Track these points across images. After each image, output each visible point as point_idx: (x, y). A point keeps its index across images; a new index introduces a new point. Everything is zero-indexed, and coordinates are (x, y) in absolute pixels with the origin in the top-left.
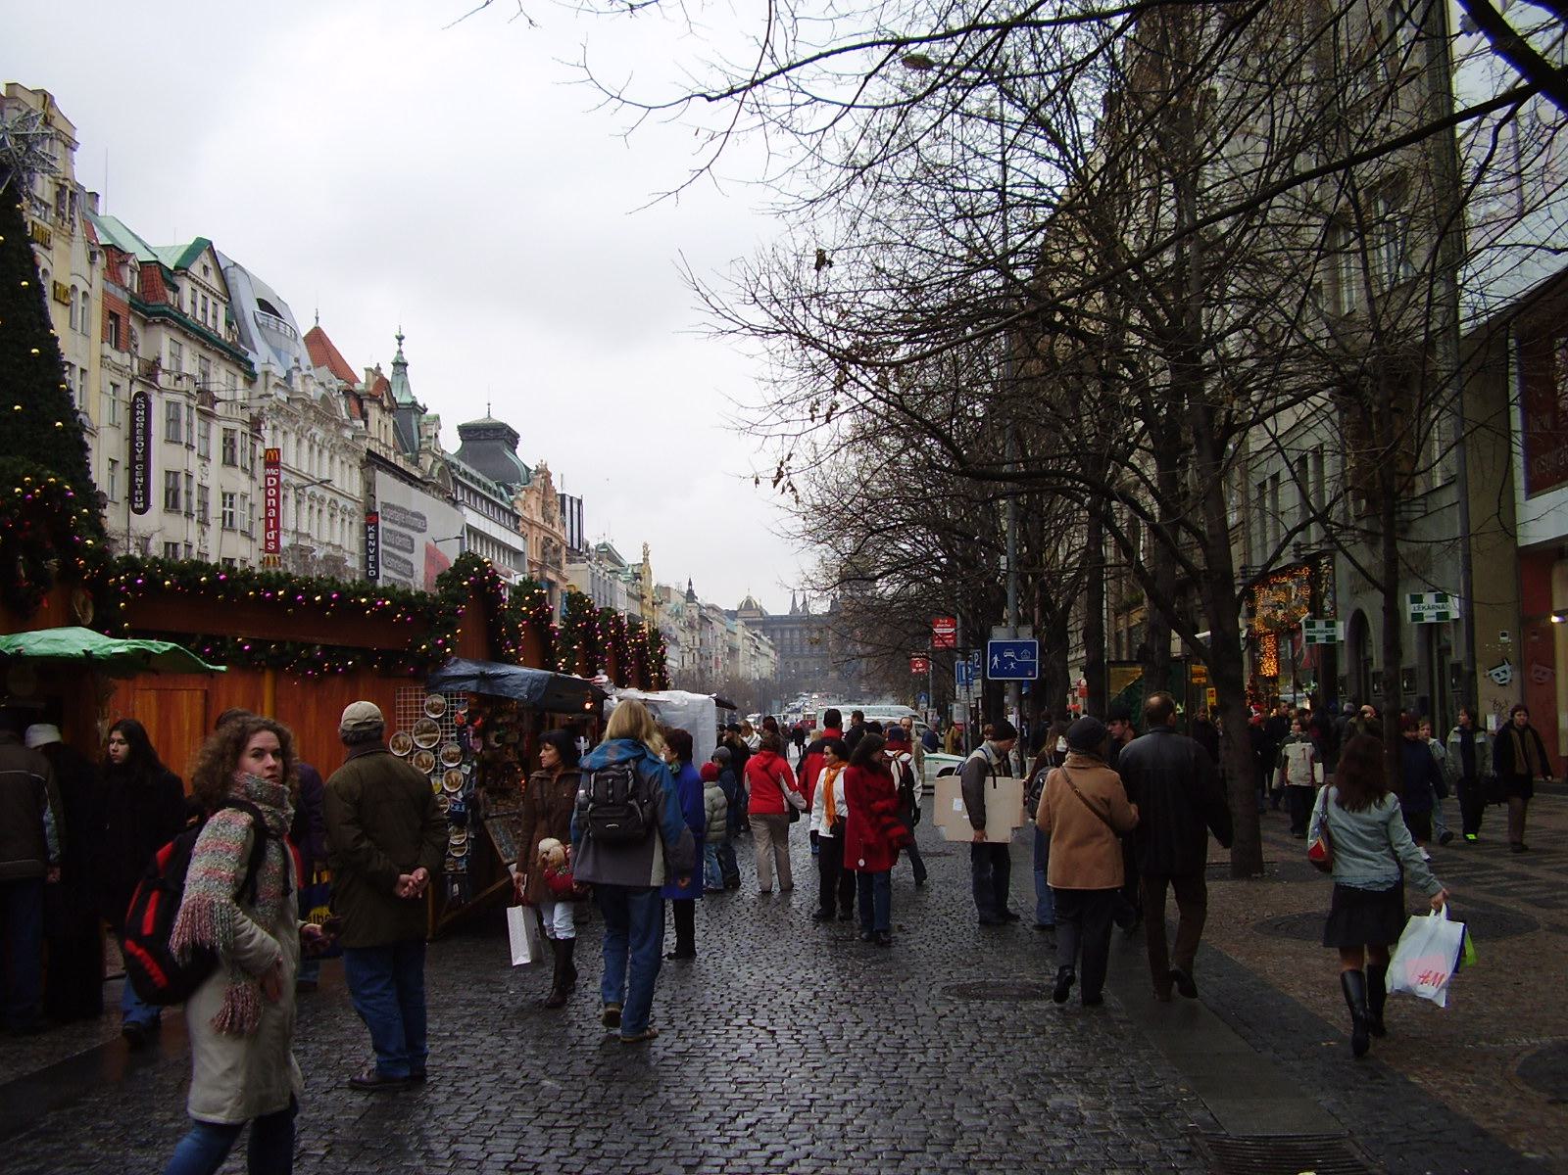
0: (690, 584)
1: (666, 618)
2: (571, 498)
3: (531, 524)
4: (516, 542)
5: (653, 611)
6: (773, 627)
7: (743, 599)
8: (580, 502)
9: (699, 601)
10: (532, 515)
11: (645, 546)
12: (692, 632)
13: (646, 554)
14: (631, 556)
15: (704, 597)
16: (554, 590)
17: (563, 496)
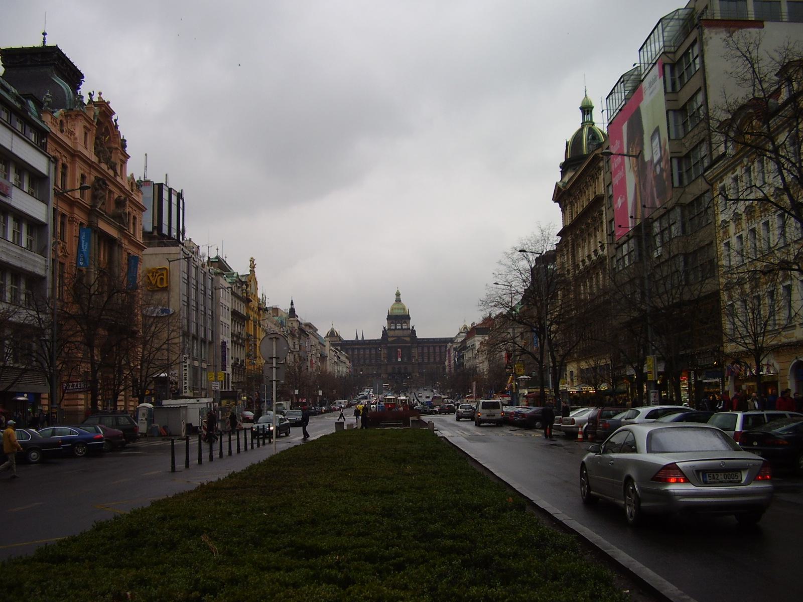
0: (292, 304)
1: (273, 326)
2: (170, 190)
3: (75, 155)
4: (39, 162)
5: (259, 315)
6: (348, 347)
7: (329, 329)
8: (180, 196)
9: (299, 319)
10: (75, 143)
11: (252, 260)
12: (293, 339)
13: (253, 267)
14: (240, 268)
15: (303, 315)
16: (116, 248)
17: (160, 186)
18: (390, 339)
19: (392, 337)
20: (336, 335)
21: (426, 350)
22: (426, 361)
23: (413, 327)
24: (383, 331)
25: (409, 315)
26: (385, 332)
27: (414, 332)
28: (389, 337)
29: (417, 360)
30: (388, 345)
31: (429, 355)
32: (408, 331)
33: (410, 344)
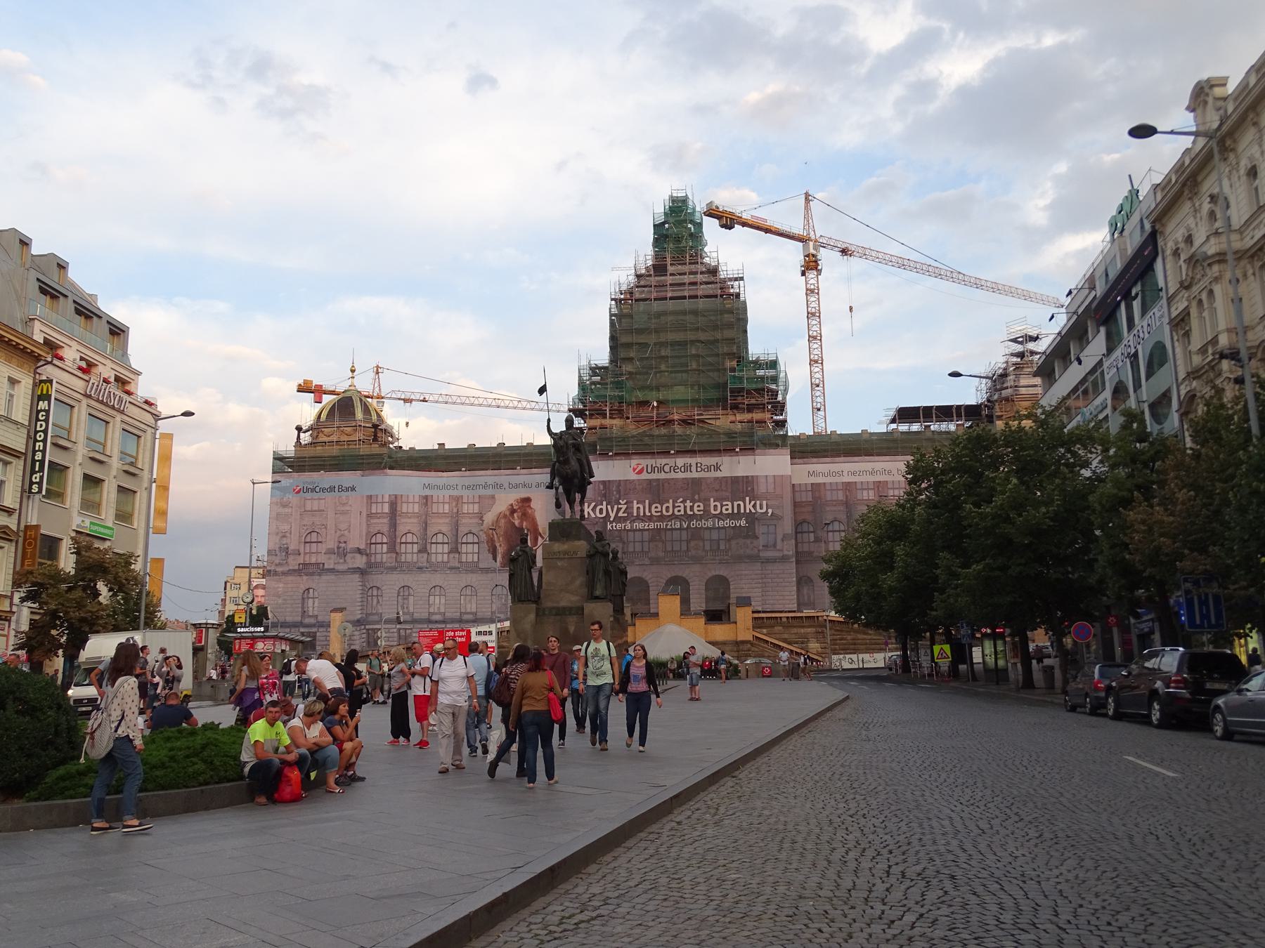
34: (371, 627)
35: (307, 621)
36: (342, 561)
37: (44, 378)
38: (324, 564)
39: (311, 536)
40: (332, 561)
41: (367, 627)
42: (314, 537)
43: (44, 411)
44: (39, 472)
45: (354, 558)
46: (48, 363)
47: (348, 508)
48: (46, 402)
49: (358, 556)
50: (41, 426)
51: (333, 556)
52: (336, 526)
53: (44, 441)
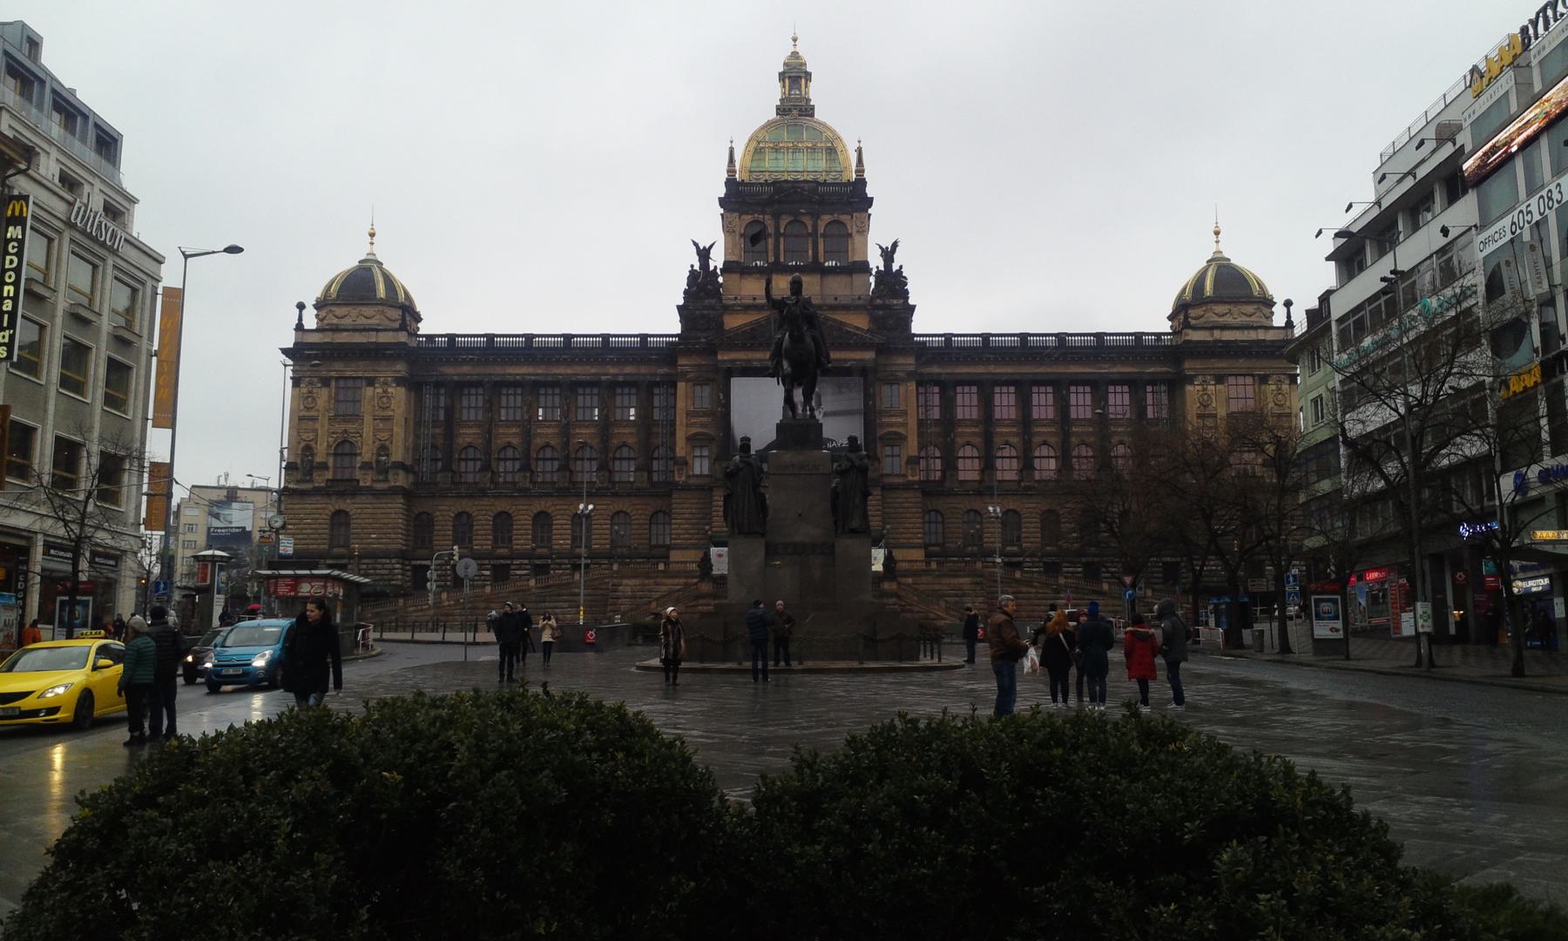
6: (451, 371)
18: (733, 322)
19: (747, 308)
20: (381, 291)
21: (967, 405)
22: (969, 470)
23: (888, 254)
24: (692, 272)
25: (861, 183)
26: (701, 286)
27: (893, 283)
28: (727, 309)
29: (914, 461)
30: (722, 356)
31: (988, 438)
32: (858, 279)
33: (869, 355)
34: (419, 562)
35: (336, 550)
36: (381, 478)
37: (16, 193)
38: (358, 481)
39: (344, 448)
40: (369, 478)
41: (413, 562)
42: (347, 449)
43: (16, 240)
44: (8, 328)
45: (397, 474)
46: (20, 172)
47: (390, 413)
48: (19, 228)
49: (402, 474)
50: (11, 262)
51: (370, 472)
52: (374, 435)
53: (16, 284)
